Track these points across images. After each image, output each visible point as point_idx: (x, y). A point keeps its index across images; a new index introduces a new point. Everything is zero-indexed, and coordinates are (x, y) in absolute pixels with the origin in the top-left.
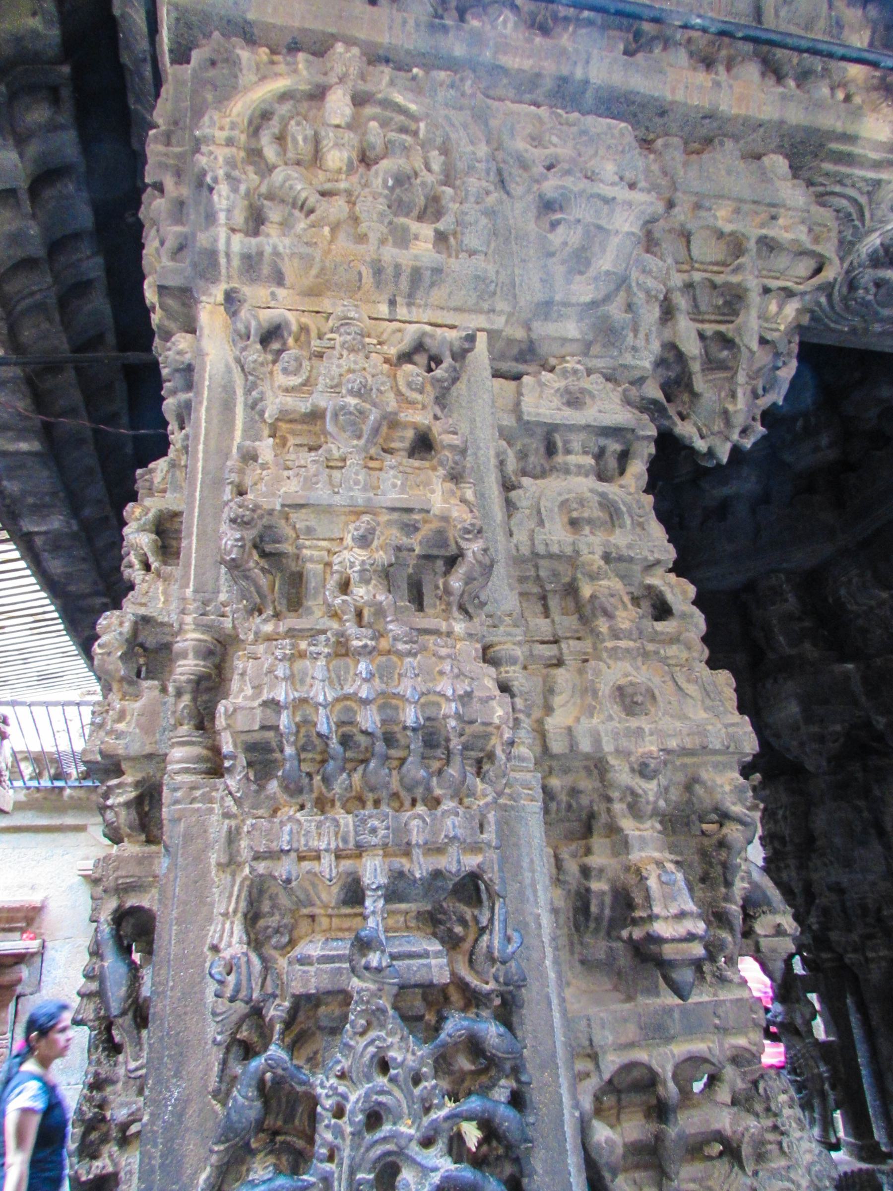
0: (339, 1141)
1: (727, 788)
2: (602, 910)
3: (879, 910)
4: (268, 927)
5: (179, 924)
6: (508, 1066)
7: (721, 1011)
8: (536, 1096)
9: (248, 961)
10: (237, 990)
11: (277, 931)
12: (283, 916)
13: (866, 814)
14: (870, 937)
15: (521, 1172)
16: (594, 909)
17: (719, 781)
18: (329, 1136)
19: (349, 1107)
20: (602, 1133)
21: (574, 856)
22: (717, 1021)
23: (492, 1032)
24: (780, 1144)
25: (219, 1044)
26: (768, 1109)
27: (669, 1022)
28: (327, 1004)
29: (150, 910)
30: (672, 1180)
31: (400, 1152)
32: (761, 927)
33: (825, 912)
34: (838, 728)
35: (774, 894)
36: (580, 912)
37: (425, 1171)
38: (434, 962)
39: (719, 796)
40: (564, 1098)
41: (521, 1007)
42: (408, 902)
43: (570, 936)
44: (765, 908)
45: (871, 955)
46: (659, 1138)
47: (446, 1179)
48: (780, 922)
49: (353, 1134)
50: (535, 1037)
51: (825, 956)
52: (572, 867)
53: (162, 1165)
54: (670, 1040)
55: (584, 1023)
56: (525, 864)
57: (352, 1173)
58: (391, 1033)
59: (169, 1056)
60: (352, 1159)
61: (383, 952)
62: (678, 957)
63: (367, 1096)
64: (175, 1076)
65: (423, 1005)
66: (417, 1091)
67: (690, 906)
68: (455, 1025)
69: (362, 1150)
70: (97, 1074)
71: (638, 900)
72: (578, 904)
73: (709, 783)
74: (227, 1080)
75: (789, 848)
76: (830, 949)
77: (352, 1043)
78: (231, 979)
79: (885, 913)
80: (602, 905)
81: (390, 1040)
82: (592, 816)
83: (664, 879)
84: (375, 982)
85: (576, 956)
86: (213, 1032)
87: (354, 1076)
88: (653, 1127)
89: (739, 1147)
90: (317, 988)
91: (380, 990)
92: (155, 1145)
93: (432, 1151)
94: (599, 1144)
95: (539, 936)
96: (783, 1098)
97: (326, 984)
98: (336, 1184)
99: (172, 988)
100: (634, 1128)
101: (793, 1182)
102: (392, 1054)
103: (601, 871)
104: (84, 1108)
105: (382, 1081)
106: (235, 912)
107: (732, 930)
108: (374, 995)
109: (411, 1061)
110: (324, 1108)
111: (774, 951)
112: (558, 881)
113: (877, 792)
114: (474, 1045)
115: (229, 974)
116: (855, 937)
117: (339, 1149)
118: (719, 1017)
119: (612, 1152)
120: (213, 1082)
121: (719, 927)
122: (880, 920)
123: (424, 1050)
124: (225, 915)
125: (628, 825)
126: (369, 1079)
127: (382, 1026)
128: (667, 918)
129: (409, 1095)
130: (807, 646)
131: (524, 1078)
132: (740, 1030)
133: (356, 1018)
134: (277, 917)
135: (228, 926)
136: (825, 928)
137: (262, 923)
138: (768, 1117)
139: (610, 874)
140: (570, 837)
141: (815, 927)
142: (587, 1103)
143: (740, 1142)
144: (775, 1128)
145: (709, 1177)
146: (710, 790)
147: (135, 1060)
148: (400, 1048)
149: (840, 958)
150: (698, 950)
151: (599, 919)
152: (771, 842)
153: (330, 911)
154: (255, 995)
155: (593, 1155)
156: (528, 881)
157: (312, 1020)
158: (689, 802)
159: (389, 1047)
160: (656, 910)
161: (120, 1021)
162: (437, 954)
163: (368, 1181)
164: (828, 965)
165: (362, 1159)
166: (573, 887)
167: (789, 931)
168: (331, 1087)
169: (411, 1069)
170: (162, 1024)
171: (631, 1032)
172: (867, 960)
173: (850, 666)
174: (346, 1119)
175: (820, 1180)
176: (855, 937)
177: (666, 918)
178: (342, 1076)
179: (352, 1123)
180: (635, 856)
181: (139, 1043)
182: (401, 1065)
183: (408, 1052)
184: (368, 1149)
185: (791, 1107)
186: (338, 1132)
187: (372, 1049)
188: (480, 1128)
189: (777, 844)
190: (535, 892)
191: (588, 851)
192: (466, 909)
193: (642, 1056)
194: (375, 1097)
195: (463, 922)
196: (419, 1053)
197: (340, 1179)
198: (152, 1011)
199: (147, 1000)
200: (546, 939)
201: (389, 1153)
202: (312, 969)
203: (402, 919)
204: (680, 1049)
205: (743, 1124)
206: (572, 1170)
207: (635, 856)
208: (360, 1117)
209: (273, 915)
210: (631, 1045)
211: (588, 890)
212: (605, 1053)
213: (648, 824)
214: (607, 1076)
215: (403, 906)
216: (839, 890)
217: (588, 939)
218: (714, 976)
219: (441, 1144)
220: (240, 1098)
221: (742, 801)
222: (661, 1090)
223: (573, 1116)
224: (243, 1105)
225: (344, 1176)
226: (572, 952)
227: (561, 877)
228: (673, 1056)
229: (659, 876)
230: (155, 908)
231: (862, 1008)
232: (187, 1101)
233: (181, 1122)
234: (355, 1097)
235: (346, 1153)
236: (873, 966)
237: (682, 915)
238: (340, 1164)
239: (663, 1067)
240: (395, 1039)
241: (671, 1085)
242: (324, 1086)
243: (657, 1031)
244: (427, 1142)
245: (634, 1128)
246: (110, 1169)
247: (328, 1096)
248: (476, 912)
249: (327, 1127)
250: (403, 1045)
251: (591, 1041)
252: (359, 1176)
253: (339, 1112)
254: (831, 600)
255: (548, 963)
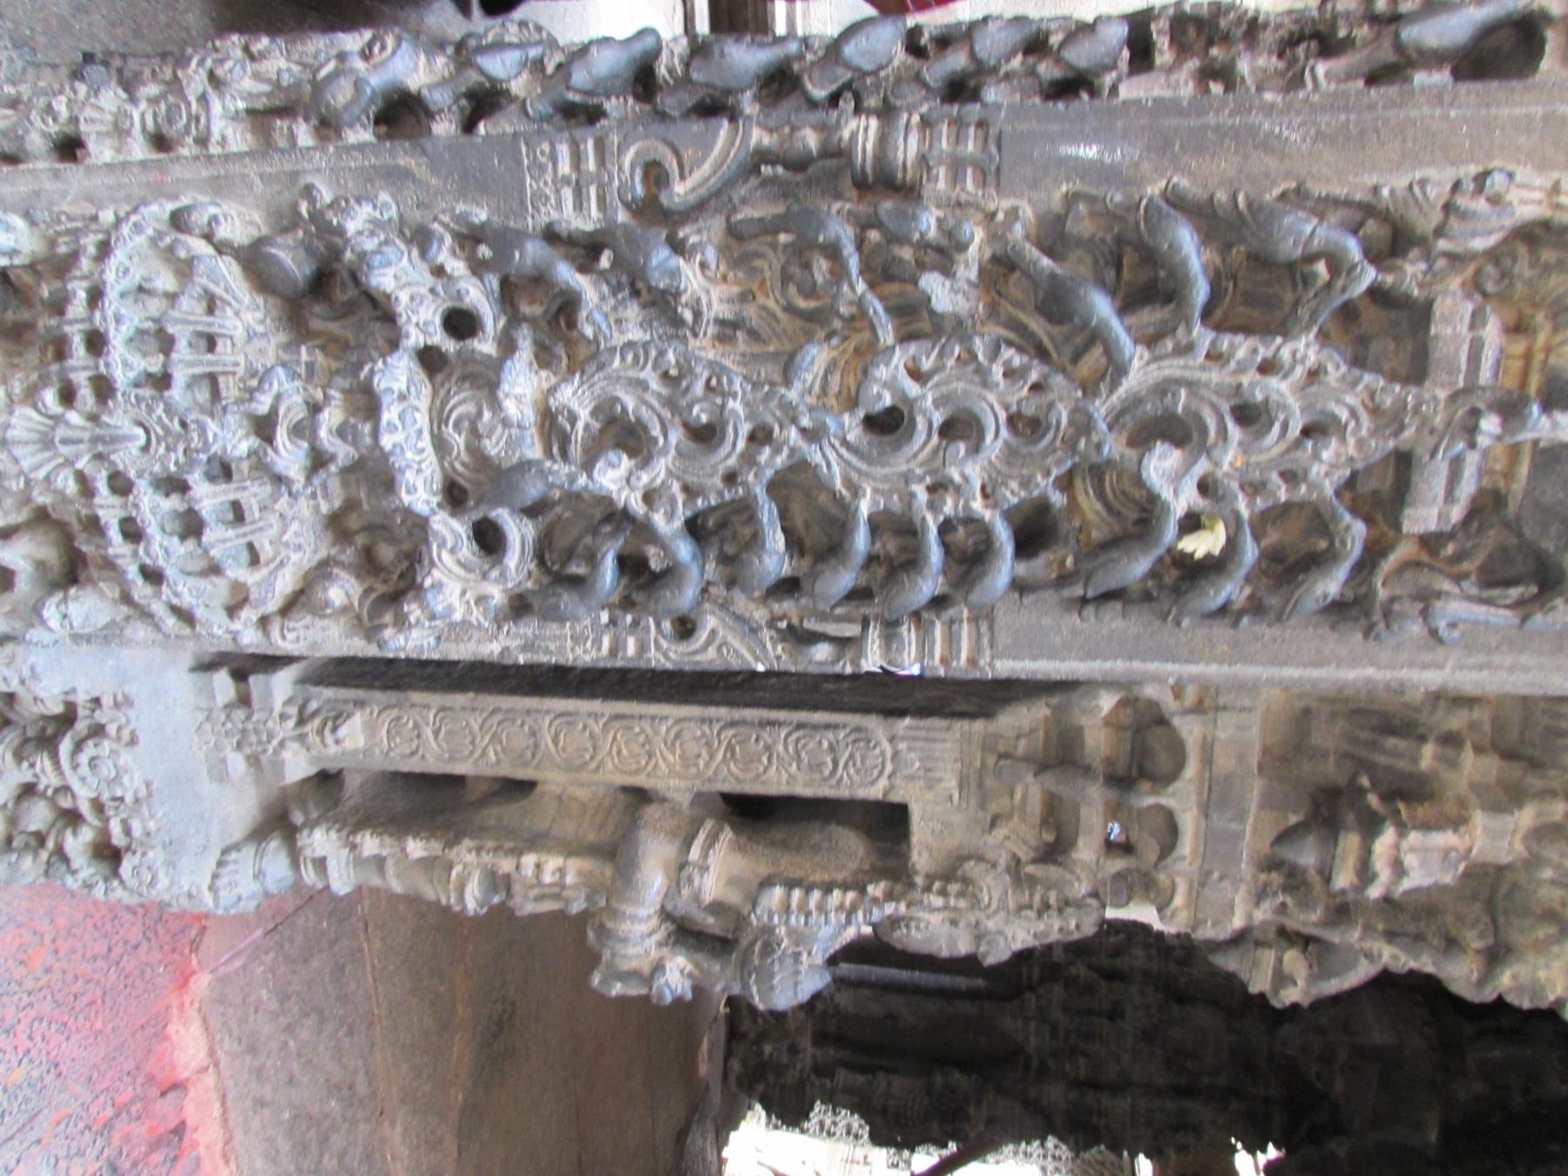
0: (1233, 365)
1: (1542, 974)
2: (1383, 751)
3: (1086, 1055)
4: (1515, 259)
5: (1546, 118)
6: (1273, 601)
7: (1227, 883)
8: (1221, 632)
9: (1490, 233)
10: (1464, 216)
11: (1505, 275)
12: (1529, 283)
13: (1206, 1080)
14: (1054, 1031)
15: (1132, 602)
16: (1391, 742)
17: (1556, 964)
18: (1241, 353)
19: (1274, 382)
20: (1107, 702)
21: (1472, 726)
22: (1216, 875)
23: (1331, 584)
24: (1030, 907)
25: (1376, 190)
26: (1067, 903)
27: (1229, 815)
28: (1397, 351)
29: (1535, 69)
30: (1035, 775)
31: (1204, 448)
32: (1293, 959)
33: (1089, 989)
34: (1339, 1086)
35: (1332, 986)
36: (1387, 720)
37: (1176, 479)
38: (1435, 511)
39: (1531, 957)
40: (1165, 663)
41: (1333, 628)
42: (1529, 477)
43: (1347, 700)
44: (1315, 969)
45: (1033, 1026)
46: (1087, 771)
47: (1166, 508)
48: (1293, 983)
49: (1239, 386)
50: (1275, 640)
51: (1036, 971)
52: (1456, 721)
53: (1204, 128)
54: (1205, 811)
55: (1247, 703)
56: (1525, 659)
57: (1190, 384)
58: (1360, 444)
59: (1348, 120)
60: (1207, 385)
61: (1499, 438)
62: (1339, 851)
63: (1284, 407)
64: (1318, 132)
65: (1384, 491)
66: (1274, 477)
67: (1406, 884)
68: (1356, 532)
69: (1214, 399)
70: (1266, 25)
71: (1422, 811)
72: (1397, 722)
73: (1555, 949)
74: (1323, 206)
75: (1173, 968)
76: (1042, 980)
77: (1360, 387)
78: (1481, 205)
79: (1082, 1061)
80: (1400, 755)
81: (1351, 441)
82: (1534, 765)
83: (1453, 854)
84: (1448, 424)
85: (1314, 705)
86: (1392, 184)
87: (1314, 389)
88: (1098, 766)
89: (1059, 864)
90: (1437, 337)
91: (1432, 432)
92: (1232, 114)
93: (1194, 492)
94: (1096, 697)
95: (1411, 665)
96: (1073, 925)
97: (1438, 353)
98: (1181, 362)
99: (1445, 117)
100: (1097, 741)
101: (995, 912)
102: (1334, 443)
103: (1454, 764)
104: (1232, 15)
105: (1295, 430)
106: (1558, 207)
107: (1316, 925)
108: (1425, 421)
109: (1316, 470)
110: (1279, 348)
111: (1255, 964)
112: (1437, 697)
113: (1235, 1105)
114: (1315, 562)
115: (1489, 199)
116: (1057, 1015)
117: (1223, 366)
118: (1222, 878)
119: (1084, 711)
120: (1317, 189)
121: (1327, 908)
122: (1073, 1051)
123: (1329, 489)
124: (1556, 189)
125: (1526, 817)
126: (1303, 410)
127: (1374, 432)
128: (1397, 847)
129: (1271, 464)
130: (1479, 1087)
131: (1245, 621)
132: (1195, 901)
133: (1392, 395)
134: (1527, 273)
135: (1537, 195)
136: (1069, 983)
137: (1522, 250)
138: (1058, 899)
139: (1447, 775)
140: (1498, 724)
141: (1073, 970)
142: (1150, 691)
143: (1066, 868)
144: (1046, 906)
145: (1023, 818)
146: (1542, 947)
147: (1327, 75)
148: (1338, 455)
149: (1031, 988)
150: (1343, 879)
151: (1373, 746)
152: (1182, 947)
153: (1539, 357)
154: (1443, 245)
155: (1083, 689)
156: (1497, 659)
157: (1388, 330)
158: (1526, 912)
159: (1343, 440)
160: (1414, 837)
161: (1387, 44)
162: (1441, 516)
163: (1175, 404)
164: (1025, 970)
165: (1202, 399)
166: (1423, 718)
167: (1282, 993)
168: (1305, 357)
169: (1306, 472)
170: (1393, 105)
171: (1224, 762)
172: (1027, 1019)
173: (1433, 1136)
174: (1258, 377)
175: (989, 943)
176: (1057, 1015)
177: (1397, 847)
178: (1314, 374)
179: (1252, 385)
180: (1479, 819)
181: (1349, 77)
182: (1316, 456)
183: (1326, 468)
184: (1214, 407)
185: (1061, 930)
186: (1241, 369)
187: (1344, 415)
188: (1208, 556)
189: (1179, 953)
190: (1480, 667)
191: (1479, 749)
192: (1477, 563)
193: (1191, 771)
194: (1281, 417)
195: (1458, 558)
196: (1327, 483)
197: (1186, 367)
198: (1494, 84)
199: (1408, 80)
200: (1404, 674)
201: (1204, 431)
202: (1463, 328)
203: (1498, 467)
204: (1188, 822)
205: (1083, 876)
206: (1108, 665)
207: (1479, 819)
208: (1259, 397)
209: (1532, 266)
210: (1207, 759)
211: (1422, 739)
212: (1204, 724)
213: (1519, 847)
214: (1177, 721)
215: (1524, 469)
216: (1115, 1014)
217: (1341, 725)
218: (1266, 885)
219: (1200, 503)
220: (1308, 229)
221: (1519, 989)
222: (1145, 786)
223: (1170, 674)
224: (1300, 233)
225: (1187, 374)
226: (1331, 701)
227: (1442, 703)
228: (1184, 811)
229: (1455, 849)
230: (1538, 77)
231: (973, 995)
232: (1283, 156)
233: (1256, 147)
234: (1280, 388)
235: (1215, 376)
236: (1020, 1022)
237: (1399, 869)
238: (1203, 368)
239: (1174, 794)
240: (1351, 449)
241: (1149, 801)
242: (1303, 348)
243: (1218, 796)
244: (1204, 487)
245: (1097, 741)
246: (1158, 60)
247: (1294, 353)
248: (1473, 577)
249: (1255, 351)
250: (1343, 459)
251: (1225, 708)
252: (1183, 393)
253: (1267, 368)
254: (1554, 1147)
255: (1370, 672)
